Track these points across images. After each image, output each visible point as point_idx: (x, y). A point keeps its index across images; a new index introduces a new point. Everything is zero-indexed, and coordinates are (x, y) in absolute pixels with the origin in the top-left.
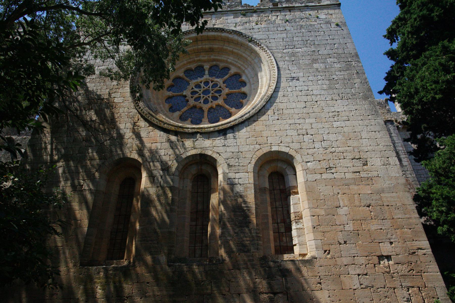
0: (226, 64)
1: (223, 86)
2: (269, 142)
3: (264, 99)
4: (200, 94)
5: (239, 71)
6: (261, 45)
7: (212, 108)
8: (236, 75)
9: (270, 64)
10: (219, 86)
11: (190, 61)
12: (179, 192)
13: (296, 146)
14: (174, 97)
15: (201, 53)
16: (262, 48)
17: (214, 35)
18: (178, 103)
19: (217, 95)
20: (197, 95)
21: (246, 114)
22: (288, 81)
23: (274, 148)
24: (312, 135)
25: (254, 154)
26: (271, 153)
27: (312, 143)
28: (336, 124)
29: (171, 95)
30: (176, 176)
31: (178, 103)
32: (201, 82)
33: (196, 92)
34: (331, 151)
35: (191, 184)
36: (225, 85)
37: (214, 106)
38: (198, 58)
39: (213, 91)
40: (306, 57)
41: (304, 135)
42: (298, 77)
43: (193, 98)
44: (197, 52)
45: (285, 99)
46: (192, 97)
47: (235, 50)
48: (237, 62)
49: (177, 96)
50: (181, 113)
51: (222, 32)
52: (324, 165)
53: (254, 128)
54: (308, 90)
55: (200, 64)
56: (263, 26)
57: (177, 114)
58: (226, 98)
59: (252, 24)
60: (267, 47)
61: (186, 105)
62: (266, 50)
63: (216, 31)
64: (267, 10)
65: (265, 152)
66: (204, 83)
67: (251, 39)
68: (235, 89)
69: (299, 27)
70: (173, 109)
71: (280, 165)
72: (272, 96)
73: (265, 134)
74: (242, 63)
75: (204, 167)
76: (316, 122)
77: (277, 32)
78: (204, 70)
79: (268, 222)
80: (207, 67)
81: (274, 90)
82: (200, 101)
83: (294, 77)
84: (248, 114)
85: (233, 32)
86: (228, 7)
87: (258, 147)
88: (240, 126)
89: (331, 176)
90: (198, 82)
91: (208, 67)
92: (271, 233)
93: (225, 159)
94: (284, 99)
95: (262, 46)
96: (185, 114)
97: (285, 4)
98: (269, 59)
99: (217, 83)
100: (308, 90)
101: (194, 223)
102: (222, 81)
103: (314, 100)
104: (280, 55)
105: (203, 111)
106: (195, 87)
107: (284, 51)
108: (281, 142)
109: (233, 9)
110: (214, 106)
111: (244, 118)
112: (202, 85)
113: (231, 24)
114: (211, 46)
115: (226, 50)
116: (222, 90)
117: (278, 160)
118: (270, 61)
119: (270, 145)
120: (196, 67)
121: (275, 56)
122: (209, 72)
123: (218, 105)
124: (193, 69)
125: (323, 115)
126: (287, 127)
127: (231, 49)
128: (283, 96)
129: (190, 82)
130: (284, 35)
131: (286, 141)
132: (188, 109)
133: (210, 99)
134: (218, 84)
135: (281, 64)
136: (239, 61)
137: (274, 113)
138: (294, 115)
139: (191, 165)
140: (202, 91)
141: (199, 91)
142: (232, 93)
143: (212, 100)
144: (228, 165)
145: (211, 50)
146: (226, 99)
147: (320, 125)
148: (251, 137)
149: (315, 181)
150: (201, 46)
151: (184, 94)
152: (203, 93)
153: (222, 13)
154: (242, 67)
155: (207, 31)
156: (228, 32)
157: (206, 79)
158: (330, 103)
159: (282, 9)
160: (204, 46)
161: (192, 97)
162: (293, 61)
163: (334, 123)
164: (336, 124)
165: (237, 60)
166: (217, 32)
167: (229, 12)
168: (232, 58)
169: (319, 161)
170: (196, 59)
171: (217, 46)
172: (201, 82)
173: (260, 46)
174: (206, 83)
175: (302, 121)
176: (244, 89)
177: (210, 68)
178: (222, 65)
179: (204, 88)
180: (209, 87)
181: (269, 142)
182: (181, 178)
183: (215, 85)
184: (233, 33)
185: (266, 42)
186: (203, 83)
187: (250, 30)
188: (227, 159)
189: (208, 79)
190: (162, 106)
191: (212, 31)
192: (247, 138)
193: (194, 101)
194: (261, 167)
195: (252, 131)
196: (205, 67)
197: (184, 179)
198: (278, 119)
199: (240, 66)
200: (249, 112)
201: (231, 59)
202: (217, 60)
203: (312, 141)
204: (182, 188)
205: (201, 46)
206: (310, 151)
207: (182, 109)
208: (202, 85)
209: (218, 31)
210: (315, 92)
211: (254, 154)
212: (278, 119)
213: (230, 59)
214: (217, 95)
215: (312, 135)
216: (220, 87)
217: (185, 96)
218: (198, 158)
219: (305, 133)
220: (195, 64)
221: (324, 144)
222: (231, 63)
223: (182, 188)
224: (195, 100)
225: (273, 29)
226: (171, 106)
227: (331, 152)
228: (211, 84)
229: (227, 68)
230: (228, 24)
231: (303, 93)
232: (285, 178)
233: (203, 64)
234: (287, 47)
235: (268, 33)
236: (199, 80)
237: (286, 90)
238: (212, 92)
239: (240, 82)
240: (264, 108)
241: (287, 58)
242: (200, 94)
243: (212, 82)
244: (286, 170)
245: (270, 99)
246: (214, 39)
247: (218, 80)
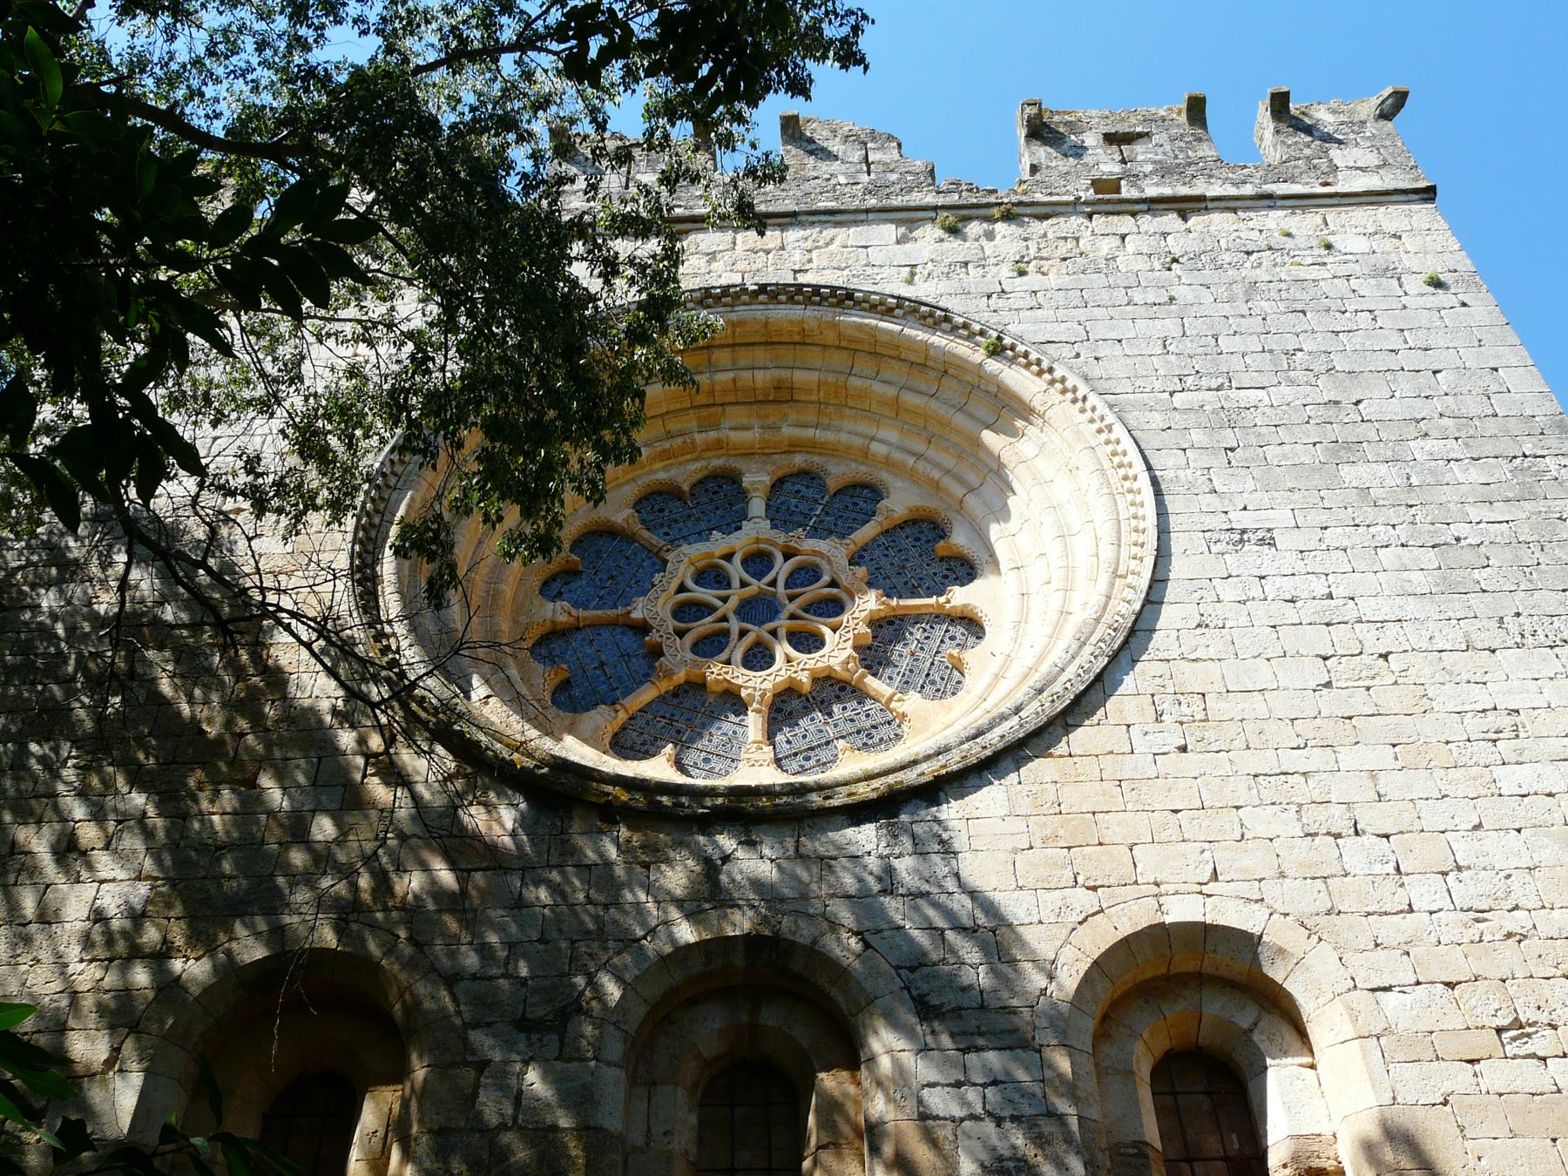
0: (863, 468)
2: (1147, 873)
3: (1093, 640)
4: (724, 619)
5: (932, 504)
6: (1051, 370)
8: (915, 522)
9: (1107, 464)
10: (826, 578)
11: (667, 445)
12: (626, 1162)
13: (1306, 898)
14: (578, 629)
15: (728, 409)
16: (1058, 386)
17: (802, 322)
18: (602, 664)
20: (706, 625)
21: (1003, 718)
22: (1214, 549)
23: (1182, 910)
24: (1387, 837)
25: (1067, 942)
26: (1159, 937)
27: (1391, 884)
28: (1510, 780)
29: (562, 618)
30: (609, 1064)
31: (602, 664)
32: (728, 557)
33: (704, 609)
34: (1511, 927)
35: (693, 1119)
36: (861, 571)
38: (713, 435)
39: (798, 601)
40: (1296, 429)
41: (1338, 836)
42: (1269, 530)
43: (689, 639)
44: (708, 406)
45: (1212, 643)
46: (681, 634)
47: (909, 398)
48: (919, 456)
49: (596, 625)
50: (622, 716)
51: (840, 303)
52: (1485, 1006)
53: (1052, 797)
54: (1330, 596)
55: (718, 463)
56: (1053, 280)
57: (604, 719)
58: (870, 641)
59: (994, 269)
60: (1086, 379)
61: (647, 675)
62: (1080, 395)
63: (808, 301)
64: (1070, 209)
65: (1127, 929)
66: (745, 562)
67: (999, 338)
68: (914, 595)
69: (1239, 290)
70: (576, 692)
71: (1215, 1007)
72: (1139, 626)
73: (1115, 828)
74: (949, 462)
75: (771, 1017)
76: (1399, 764)
77: (1129, 308)
78: (743, 495)
80: (757, 479)
81: (1148, 594)
82: (724, 656)
83: (1244, 531)
84: (1015, 721)
85: (899, 306)
86: (867, 192)
87: (1084, 900)
88: (972, 781)
89: (1530, 1076)
90: (711, 555)
91: (767, 480)
93: (897, 968)
94: (1203, 641)
95: (1058, 374)
96: (640, 722)
97: (1157, 184)
98: (1104, 436)
99: (818, 560)
100: (1330, 596)
102: (844, 551)
103: (1367, 650)
104: (1158, 420)
106: (697, 583)
107: (1178, 400)
108: (1215, 876)
109: (896, 201)
112: (736, 570)
113: (886, 272)
114: (786, 374)
115: (863, 395)
116: (844, 596)
117: (1200, 980)
118: (1110, 448)
119: (1155, 890)
120: (700, 482)
121: (1132, 423)
122: (768, 507)
124: (686, 488)
125: (1428, 728)
126: (1239, 790)
127: (891, 392)
128: (1199, 626)
129: (670, 557)
130: (1171, 327)
131: (1246, 870)
132: (662, 699)
133: (782, 649)
134: (824, 564)
135: (1170, 462)
136: (932, 453)
137: (1159, 717)
138: (1271, 727)
139: (693, 1002)
140: (733, 602)
141: (719, 603)
142: (902, 618)
145: (783, 395)
146: (869, 648)
147: (1422, 784)
148: (1037, 843)
149: (1445, 1103)
150: (731, 375)
151: (637, 615)
152: (738, 612)
153: (838, 218)
154: (947, 482)
155: (762, 297)
156: (873, 308)
157: (758, 541)
158: (1464, 664)
159: (1145, 207)
160: (747, 375)
161: (681, 634)
162: (1232, 450)
163: (1499, 772)
164: (1510, 780)
165: (920, 447)
166: (814, 304)
167: (871, 216)
168: (893, 436)
169: (1450, 985)
170: (699, 438)
171: (813, 377)
172: (728, 557)
173: (1047, 376)
174: (758, 561)
175: (1315, 759)
176: (959, 597)
177: (773, 486)
178: (838, 473)
179: (744, 584)
180: (773, 583)
181: (1147, 873)
182: (633, 1081)
183: (806, 574)
184: (897, 311)
185: (1078, 355)
186: (737, 559)
187: (989, 297)
188: (912, 969)
189: (766, 541)
190: (514, 673)
191: (791, 300)
192: (1015, 851)
193: (690, 656)
194: (1105, 1018)
195: (1044, 810)
196: (747, 481)
197: (654, 1084)
198: (1183, 749)
199: (936, 474)
200: (1018, 710)
201: (886, 439)
202: (812, 447)
203: (1390, 868)
204: (639, 1141)
205: (731, 375)
206: (1391, 927)
207: (626, 694)
208: (736, 570)
209: (824, 298)
210: (1368, 608)
211: (1067, 942)
212: (1183, 749)
213: (882, 442)
215: (1387, 837)
216: (833, 584)
217: (643, 628)
218: (739, 960)
219: (1345, 827)
220: (698, 465)
221: (1467, 890)
222: (888, 463)
223: (639, 1141)
224: (696, 648)
225: (1105, 295)
226: (563, 676)
227: (1509, 935)
228: (782, 569)
229: (864, 486)
230: (869, 271)
231: (1307, 611)
232: (1251, 1086)
233: (734, 463)
234: (1190, 380)
235: (1082, 314)
236: (718, 544)
237: (1211, 597)
238: (792, 607)
239: (942, 559)
240: (1099, 686)
241: (1197, 436)
242: (724, 619)
243: (787, 557)
244: (1256, 1037)
245: (1126, 642)
246: (797, 338)
247: (822, 545)
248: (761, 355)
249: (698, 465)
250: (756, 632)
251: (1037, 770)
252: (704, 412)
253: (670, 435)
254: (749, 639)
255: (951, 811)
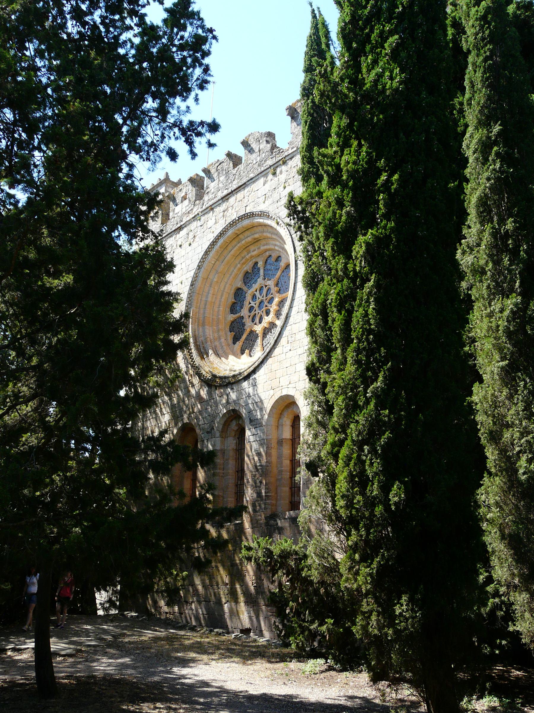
23: (284, 393)
144: (250, 419)
153: (254, 180)
190: (223, 340)
198: (290, 350)
212: (290, 350)
220: (251, 263)
248: (247, 233)
249: (251, 263)
250: (264, 309)
251: (270, 361)
252: (246, 250)
253: (243, 258)
254: (264, 311)
255: (256, 376)
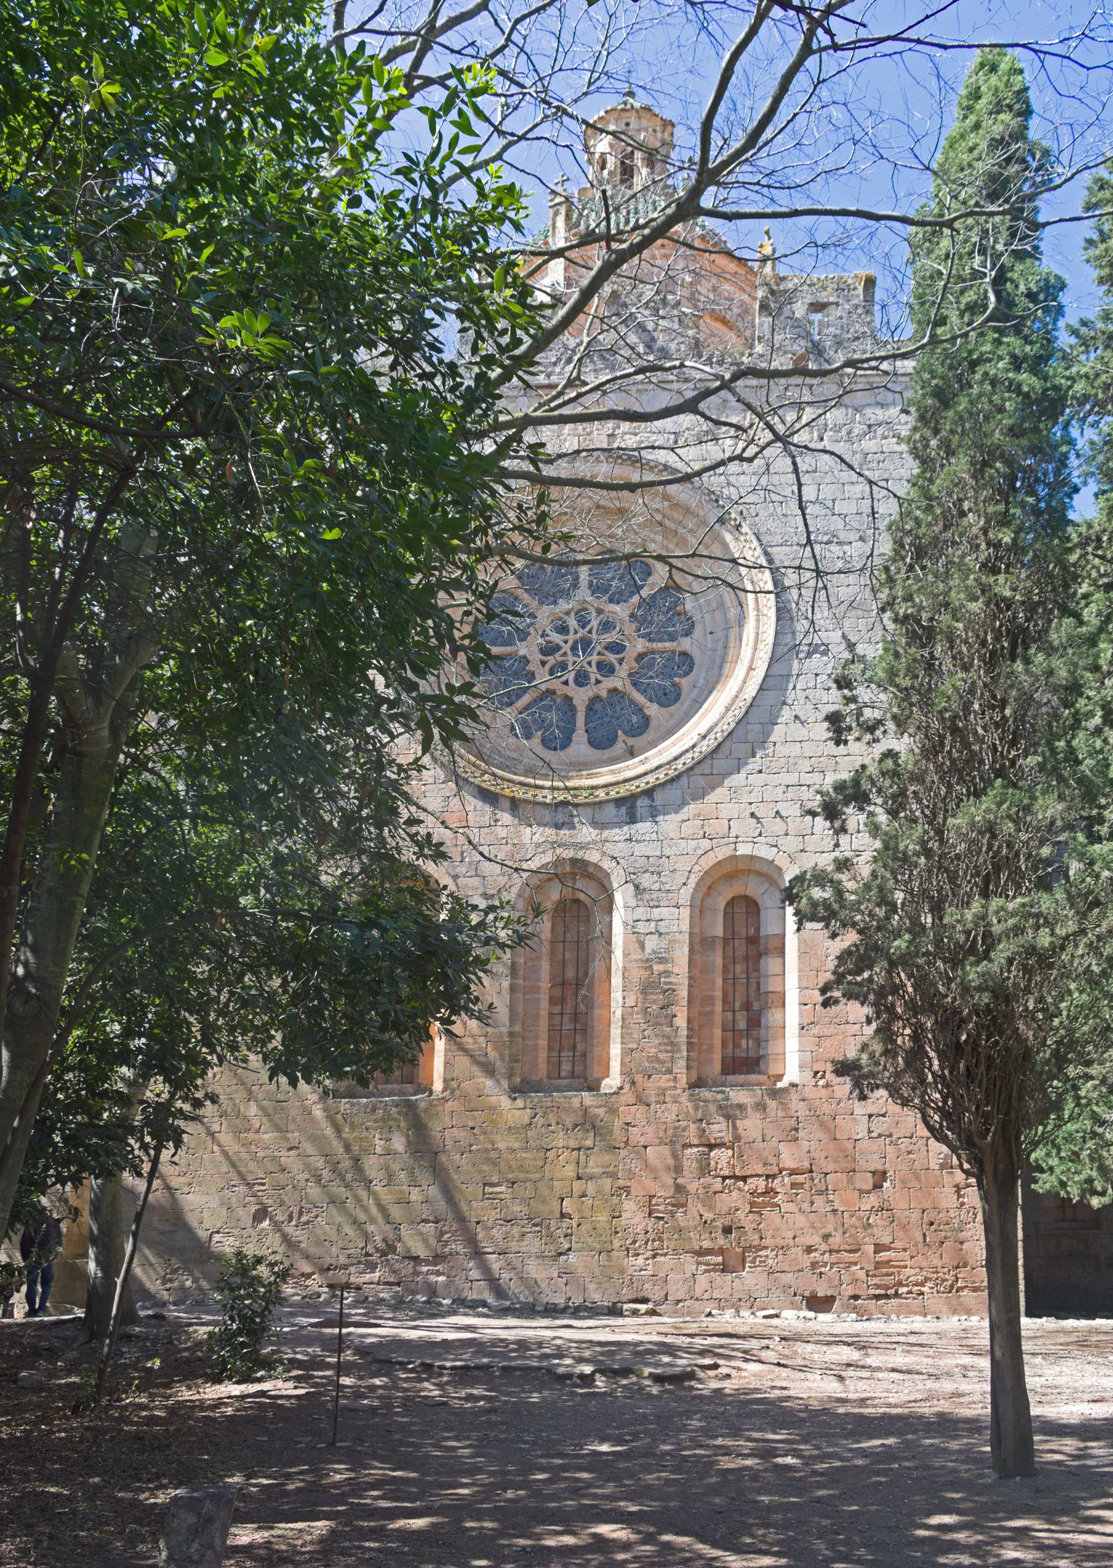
1: (630, 628)
7: (597, 698)
19: (612, 658)
23: (743, 850)
26: (733, 858)
37: (604, 694)
43: (548, 666)
79: (713, 1012)
92: (718, 1032)
101: (557, 1009)
105: (573, 709)
108: (760, 835)
110: (604, 694)
111: (680, 765)
123: (614, 691)
143: (599, 677)
151: (522, 652)
180: (590, 632)
198: (760, 772)
214: (612, 658)
247: (617, 608)
